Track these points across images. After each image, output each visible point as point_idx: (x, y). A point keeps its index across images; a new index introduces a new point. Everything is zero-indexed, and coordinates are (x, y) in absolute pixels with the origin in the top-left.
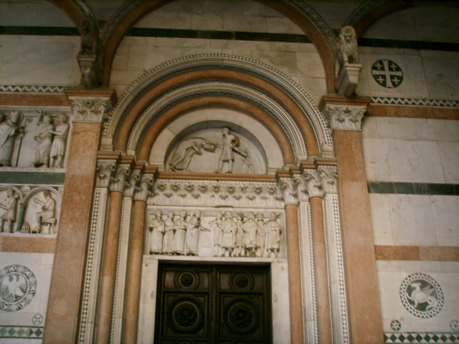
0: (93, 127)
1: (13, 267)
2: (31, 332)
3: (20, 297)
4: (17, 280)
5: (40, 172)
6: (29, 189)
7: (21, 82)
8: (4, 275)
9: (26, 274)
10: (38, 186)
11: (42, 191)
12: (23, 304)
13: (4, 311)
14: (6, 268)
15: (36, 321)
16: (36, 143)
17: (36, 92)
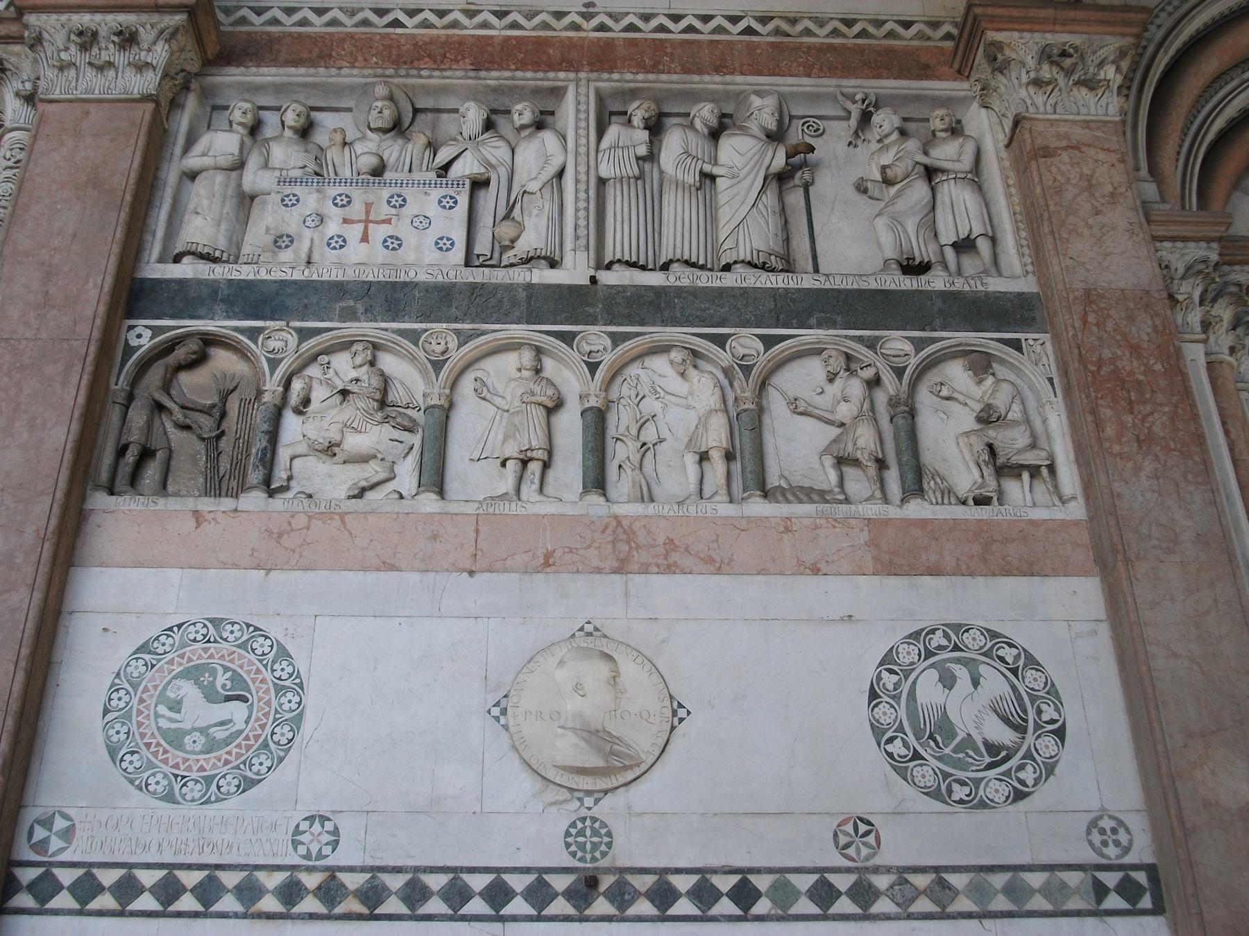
0: (1099, 134)
1: (939, 633)
2: (1101, 891)
3: (1008, 748)
4: (976, 683)
5: (930, 288)
6: (908, 347)
8: (912, 663)
9: (1002, 659)
10: (943, 339)
12: (1028, 775)
13: (958, 808)
14: (915, 635)
15: (1105, 843)
17: (821, 36)
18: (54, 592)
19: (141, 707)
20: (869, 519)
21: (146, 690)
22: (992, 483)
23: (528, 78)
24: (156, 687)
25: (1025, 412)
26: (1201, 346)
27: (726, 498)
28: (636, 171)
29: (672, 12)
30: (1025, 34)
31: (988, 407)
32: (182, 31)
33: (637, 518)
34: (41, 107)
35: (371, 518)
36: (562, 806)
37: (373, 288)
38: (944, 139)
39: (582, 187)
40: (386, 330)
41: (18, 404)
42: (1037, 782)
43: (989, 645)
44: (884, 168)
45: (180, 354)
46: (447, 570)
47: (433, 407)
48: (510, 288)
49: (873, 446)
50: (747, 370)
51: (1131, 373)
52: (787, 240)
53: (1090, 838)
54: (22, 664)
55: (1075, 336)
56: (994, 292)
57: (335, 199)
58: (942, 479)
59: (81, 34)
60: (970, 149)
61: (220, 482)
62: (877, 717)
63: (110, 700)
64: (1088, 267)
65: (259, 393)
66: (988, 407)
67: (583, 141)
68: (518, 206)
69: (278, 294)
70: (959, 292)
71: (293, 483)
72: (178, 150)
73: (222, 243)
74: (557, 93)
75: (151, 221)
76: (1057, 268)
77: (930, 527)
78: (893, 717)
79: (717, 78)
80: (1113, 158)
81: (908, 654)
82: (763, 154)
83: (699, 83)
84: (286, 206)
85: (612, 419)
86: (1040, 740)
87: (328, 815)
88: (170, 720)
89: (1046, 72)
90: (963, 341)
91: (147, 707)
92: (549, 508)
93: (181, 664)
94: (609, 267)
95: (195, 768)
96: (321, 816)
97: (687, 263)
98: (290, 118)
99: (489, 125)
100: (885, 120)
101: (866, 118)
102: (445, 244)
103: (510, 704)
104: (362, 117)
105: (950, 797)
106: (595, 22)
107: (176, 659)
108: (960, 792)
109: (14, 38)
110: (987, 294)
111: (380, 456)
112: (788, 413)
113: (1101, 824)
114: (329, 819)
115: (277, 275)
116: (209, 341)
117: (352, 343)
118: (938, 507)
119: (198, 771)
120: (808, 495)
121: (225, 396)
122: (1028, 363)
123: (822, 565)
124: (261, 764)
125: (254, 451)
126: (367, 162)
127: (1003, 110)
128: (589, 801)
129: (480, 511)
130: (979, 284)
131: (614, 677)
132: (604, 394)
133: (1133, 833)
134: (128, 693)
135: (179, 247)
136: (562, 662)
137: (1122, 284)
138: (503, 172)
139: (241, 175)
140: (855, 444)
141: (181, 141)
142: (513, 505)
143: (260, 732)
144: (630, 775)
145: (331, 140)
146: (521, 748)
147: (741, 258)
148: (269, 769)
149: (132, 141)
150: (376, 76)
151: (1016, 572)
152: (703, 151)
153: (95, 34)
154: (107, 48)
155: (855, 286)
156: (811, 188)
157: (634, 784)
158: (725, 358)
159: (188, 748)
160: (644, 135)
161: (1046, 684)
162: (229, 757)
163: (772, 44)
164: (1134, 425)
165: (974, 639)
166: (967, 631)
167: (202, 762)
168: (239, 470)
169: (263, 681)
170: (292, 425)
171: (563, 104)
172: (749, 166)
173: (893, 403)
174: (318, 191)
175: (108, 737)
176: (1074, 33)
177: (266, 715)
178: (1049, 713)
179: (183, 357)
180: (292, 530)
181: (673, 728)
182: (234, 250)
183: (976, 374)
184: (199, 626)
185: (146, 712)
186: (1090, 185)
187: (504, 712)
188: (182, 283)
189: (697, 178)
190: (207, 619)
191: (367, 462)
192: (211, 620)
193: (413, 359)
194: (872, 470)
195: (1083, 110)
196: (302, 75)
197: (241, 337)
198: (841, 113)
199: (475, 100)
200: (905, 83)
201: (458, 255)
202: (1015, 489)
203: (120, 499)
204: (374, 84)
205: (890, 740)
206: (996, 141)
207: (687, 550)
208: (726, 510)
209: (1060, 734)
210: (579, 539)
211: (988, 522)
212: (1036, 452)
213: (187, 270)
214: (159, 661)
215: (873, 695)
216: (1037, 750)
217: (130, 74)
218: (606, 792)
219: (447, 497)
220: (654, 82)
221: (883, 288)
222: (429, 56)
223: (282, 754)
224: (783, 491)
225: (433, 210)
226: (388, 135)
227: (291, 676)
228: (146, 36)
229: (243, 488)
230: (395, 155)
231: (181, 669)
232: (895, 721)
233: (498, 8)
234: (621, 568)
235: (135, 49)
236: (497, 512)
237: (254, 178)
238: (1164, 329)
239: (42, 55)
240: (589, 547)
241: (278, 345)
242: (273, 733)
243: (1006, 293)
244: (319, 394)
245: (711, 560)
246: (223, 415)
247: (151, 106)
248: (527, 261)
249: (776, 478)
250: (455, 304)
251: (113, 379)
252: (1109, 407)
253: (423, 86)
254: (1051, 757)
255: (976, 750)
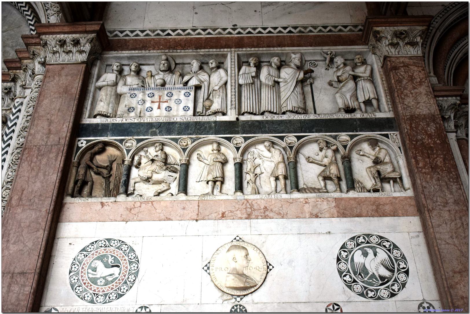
1: (362, 237)
4: (375, 255)
6: (348, 138)
7: (294, 24)
8: (352, 248)
9: (385, 246)
10: (360, 135)
11: (365, 141)
12: (396, 287)
13: (370, 300)
14: (353, 238)
16: (332, 90)
17: (315, 32)
18: (52, 230)
19: (82, 270)
20: (335, 198)
21: (84, 264)
22: (379, 184)
23: (213, 51)
24: (88, 263)
25: (391, 159)
26: (454, 134)
27: (284, 192)
28: (252, 81)
29: (264, 26)
30: (387, 28)
31: (377, 158)
32: (94, 40)
33: (254, 200)
34: (47, 67)
35: (162, 203)
36: (229, 301)
37: (162, 124)
38: (359, 66)
39: (233, 87)
40: (167, 138)
41: (40, 167)
42: (399, 290)
43: (380, 241)
44: (338, 77)
45: (96, 149)
46: (188, 220)
47: (183, 164)
48: (209, 123)
49: (336, 173)
50: (291, 148)
51: (429, 144)
52: (305, 103)
53: (419, 310)
54: (41, 256)
55: (407, 132)
56: (378, 118)
57: (149, 95)
58: (361, 183)
59: (60, 41)
60: (369, 68)
61: (110, 192)
62: (340, 267)
63: (72, 268)
64: (411, 107)
65: (123, 161)
66: (377, 158)
67: (233, 72)
68: (211, 95)
69: (129, 127)
70: (366, 118)
71: (135, 192)
72: (94, 80)
73: (110, 111)
74: (225, 56)
75: (86, 104)
76: (400, 108)
77: (357, 200)
78: (346, 267)
79: (279, 48)
80: (420, 69)
81: (351, 245)
82: (295, 73)
83: (273, 50)
84: (132, 97)
85: (245, 167)
86: (399, 275)
87: (148, 306)
88: (93, 274)
89: (395, 41)
90: (367, 135)
91: (85, 270)
92: (223, 197)
93: (96, 255)
94: (243, 114)
95: (101, 291)
96: (145, 307)
97: (270, 112)
98: (133, 68)
99: (201, 68)
100: (339, 60)
101: (332, 60)
102: (186, 109)
103: (211, 265)
104: (157, 67)
105: (367, 296)
106: (237, 31)
107: (95, 253)
108: (371, 294)
109: (38, 44)
110: (376, 119)
111: (165, 181)
112: (306, 162)
113: (423, 305)
114: (148, 308)
115: (129, 121)
116: (106, 144)
117: (155, 143)
118: (360, 193)
119: (102, 292)
120: (313, 190)
121: (112, 162)
122: (391, 142)
123: (320, 215)
124: (124, 289)
125: (122, 181)
126: (159, 82)
127: (380, 55)
128: (239, 299)
129: (200, 199)
130: (373, 115)
131: (247, 255)
132: (242, 158)
133: (435, 308)
134: (78, 265)
135: (96, 113)
136: (228, 250)
137: (424, 113)
138: (206, 84)
139: (117, 88)
140: (330, 172)
141: (95, 77)
142: (211, 196)
143: (124, 277)
144: (253, 290)
145: (147, 75)
146: (214, 281)
147: (289, 109)
148: (127, 290)
149: (79, 77)
150: (162, 53)
151: (389, 215)
152: (275, 74)
153: (65, 41)
154: (69, 46)
155: (329, 118)
156: (313, 85)
157: (254, 293)
158: (284, 144)
159: (99, 284)
160: (254, 69)
161: (401, 255)
162: (113, 287)
163: (298, 36)
164: (430, 163)
165: (374, 239)
166: (372, 236)
167: (103, 289)
168: (117, 187)
169: (125, 260)
170: (135, 172)
171: (226, 60)
172: (291, 78)
173: (343, 158)
174: (143, 92)
175: (71, 281)
176: (405, 26)
177: (126, 272)
178: (402, 265)
179: (97, 150)
180: (135, 208)
181: (268, 273)
182: (114, 113)
183: (372, 147)
184: (103, 241)
185: (84, 272)
186: (411, 79)
187: (208, 268)
188: (97, 125)
189: (273, 83)
190: (106, 239)
191: (161, 184)
192: (107, 239)
193: (176, 148)
194: (336, 181)
195: (409, 53)
196: (136, 53)
197: (117, 142)
198: (323, 59)
199: (197, 60)
200: (345, 47)
201: (191, 112)
202: (387, 186)
203: (76, 199)
204: (161, 55)
205: (345, 276)
206: (378, 66)
207: (271, 210)
208: (285, 196)
209: (407, 272)
210: (234, 208)
211: (378, 198)
212: (394, 173)
213: (98, 120)
214: (89, 254)
215: (338, 260)
216: (398, 279)
217: (77, 54)
218: (245, 296)
219: (188, 195)
220: (257, 51)
221: (339, 118)
222: (180, 45)
223: (131, 285)
224: (305, 189)
225: (182, 97)
226: (167, 73)
227: (135, 258)
228: (83, 41)
229: (118, 194)
230: (169, 79)
231: (97, 256)
232: (346, 269)
233: (203, 28)
234: (249, 217)
235: (79, 46)
236: (205, 199)
237: (121, 89)
238: (440, 128)
239: (47, 49)
240: (237, 210)
241: (130, 144)
242: (128, 278)
243: (383, 118)
244: (144, 161)
245: (279, 214)
246: (111, 169)
247: (85, 65)
248: (215, 113)
249: (303, 185)
250: (190, 128)
251: (73, 158)
252: (420, 156)
253: (178, 56)
254: (404, 281)
255: (376, 279)
